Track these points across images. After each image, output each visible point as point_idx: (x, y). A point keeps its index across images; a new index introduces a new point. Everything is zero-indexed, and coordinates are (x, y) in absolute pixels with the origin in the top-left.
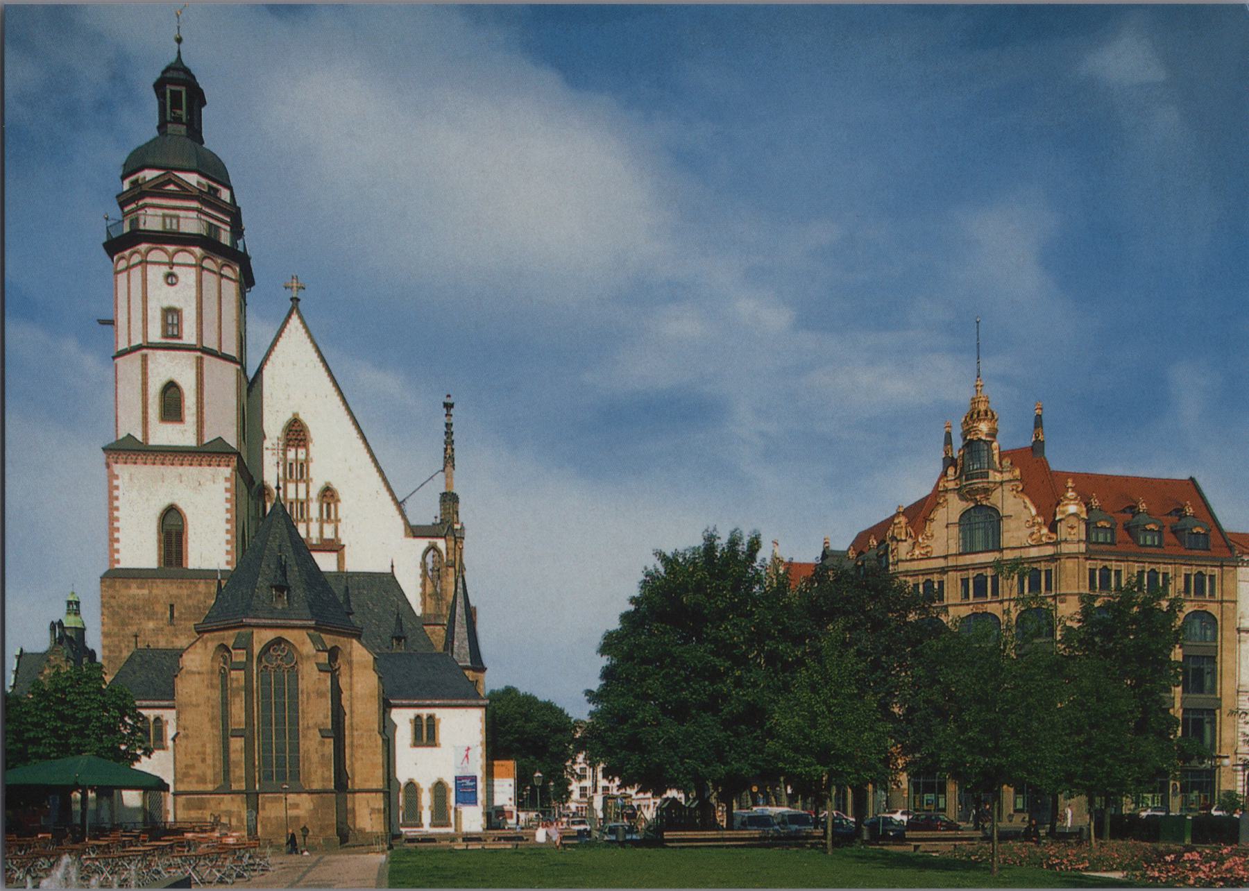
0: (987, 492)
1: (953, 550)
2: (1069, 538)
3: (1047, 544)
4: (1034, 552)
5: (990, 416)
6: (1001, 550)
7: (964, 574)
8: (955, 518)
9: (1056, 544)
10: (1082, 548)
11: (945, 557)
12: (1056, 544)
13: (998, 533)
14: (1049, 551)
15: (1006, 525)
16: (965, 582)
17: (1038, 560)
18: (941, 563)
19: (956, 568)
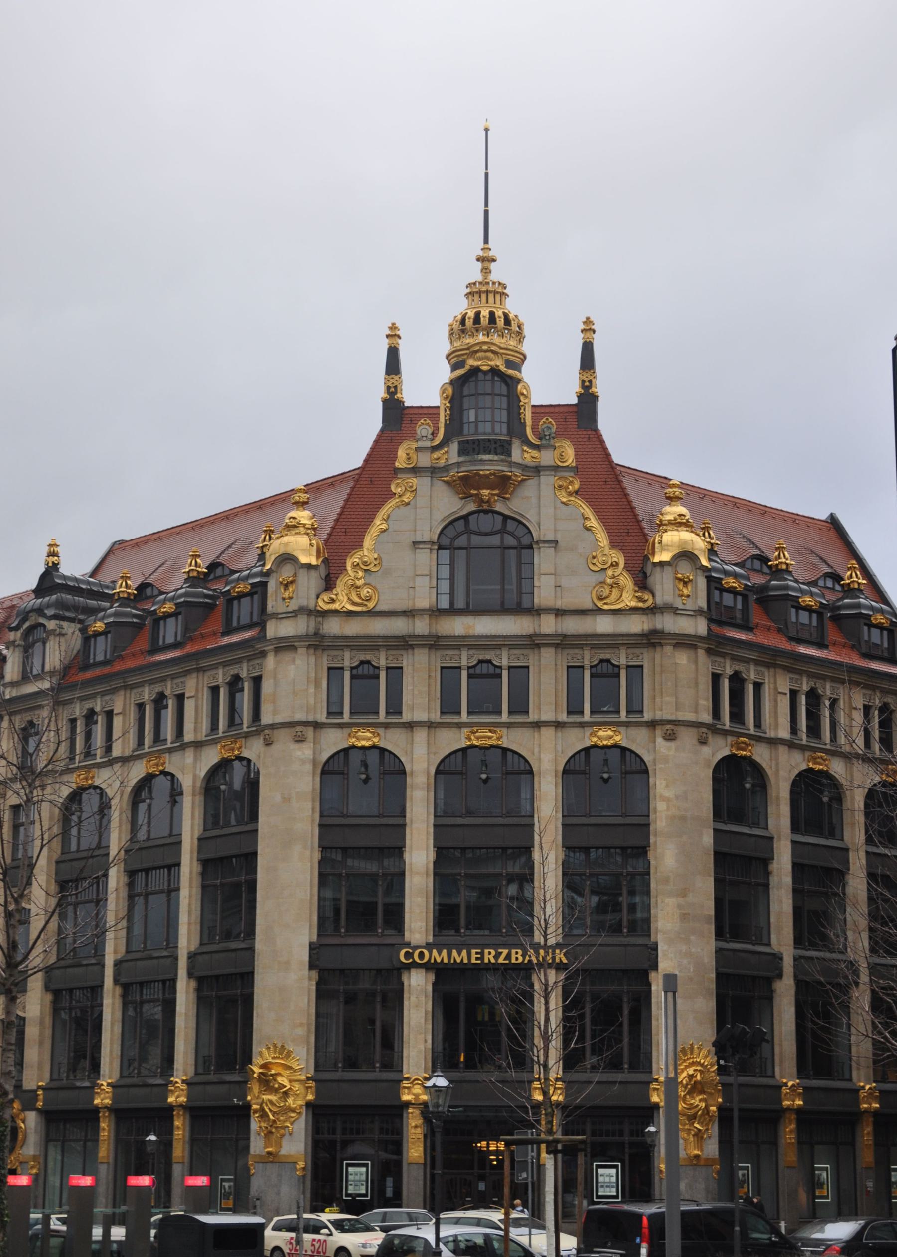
0: (503, 484)
1: (423, 602)
2: (678, 604)
3: (634, 610)
4: (604, 625)
5: (501, 322)
7: (450, 658)
9: (653, 610)
11: (410, 614)
12: (653, 610)
13: (525, 577)
14: (636, 625)
15: (543, 560)
16: (449, 673)
17: (614, 641)
18: (398, 626)
19: (435, 643)
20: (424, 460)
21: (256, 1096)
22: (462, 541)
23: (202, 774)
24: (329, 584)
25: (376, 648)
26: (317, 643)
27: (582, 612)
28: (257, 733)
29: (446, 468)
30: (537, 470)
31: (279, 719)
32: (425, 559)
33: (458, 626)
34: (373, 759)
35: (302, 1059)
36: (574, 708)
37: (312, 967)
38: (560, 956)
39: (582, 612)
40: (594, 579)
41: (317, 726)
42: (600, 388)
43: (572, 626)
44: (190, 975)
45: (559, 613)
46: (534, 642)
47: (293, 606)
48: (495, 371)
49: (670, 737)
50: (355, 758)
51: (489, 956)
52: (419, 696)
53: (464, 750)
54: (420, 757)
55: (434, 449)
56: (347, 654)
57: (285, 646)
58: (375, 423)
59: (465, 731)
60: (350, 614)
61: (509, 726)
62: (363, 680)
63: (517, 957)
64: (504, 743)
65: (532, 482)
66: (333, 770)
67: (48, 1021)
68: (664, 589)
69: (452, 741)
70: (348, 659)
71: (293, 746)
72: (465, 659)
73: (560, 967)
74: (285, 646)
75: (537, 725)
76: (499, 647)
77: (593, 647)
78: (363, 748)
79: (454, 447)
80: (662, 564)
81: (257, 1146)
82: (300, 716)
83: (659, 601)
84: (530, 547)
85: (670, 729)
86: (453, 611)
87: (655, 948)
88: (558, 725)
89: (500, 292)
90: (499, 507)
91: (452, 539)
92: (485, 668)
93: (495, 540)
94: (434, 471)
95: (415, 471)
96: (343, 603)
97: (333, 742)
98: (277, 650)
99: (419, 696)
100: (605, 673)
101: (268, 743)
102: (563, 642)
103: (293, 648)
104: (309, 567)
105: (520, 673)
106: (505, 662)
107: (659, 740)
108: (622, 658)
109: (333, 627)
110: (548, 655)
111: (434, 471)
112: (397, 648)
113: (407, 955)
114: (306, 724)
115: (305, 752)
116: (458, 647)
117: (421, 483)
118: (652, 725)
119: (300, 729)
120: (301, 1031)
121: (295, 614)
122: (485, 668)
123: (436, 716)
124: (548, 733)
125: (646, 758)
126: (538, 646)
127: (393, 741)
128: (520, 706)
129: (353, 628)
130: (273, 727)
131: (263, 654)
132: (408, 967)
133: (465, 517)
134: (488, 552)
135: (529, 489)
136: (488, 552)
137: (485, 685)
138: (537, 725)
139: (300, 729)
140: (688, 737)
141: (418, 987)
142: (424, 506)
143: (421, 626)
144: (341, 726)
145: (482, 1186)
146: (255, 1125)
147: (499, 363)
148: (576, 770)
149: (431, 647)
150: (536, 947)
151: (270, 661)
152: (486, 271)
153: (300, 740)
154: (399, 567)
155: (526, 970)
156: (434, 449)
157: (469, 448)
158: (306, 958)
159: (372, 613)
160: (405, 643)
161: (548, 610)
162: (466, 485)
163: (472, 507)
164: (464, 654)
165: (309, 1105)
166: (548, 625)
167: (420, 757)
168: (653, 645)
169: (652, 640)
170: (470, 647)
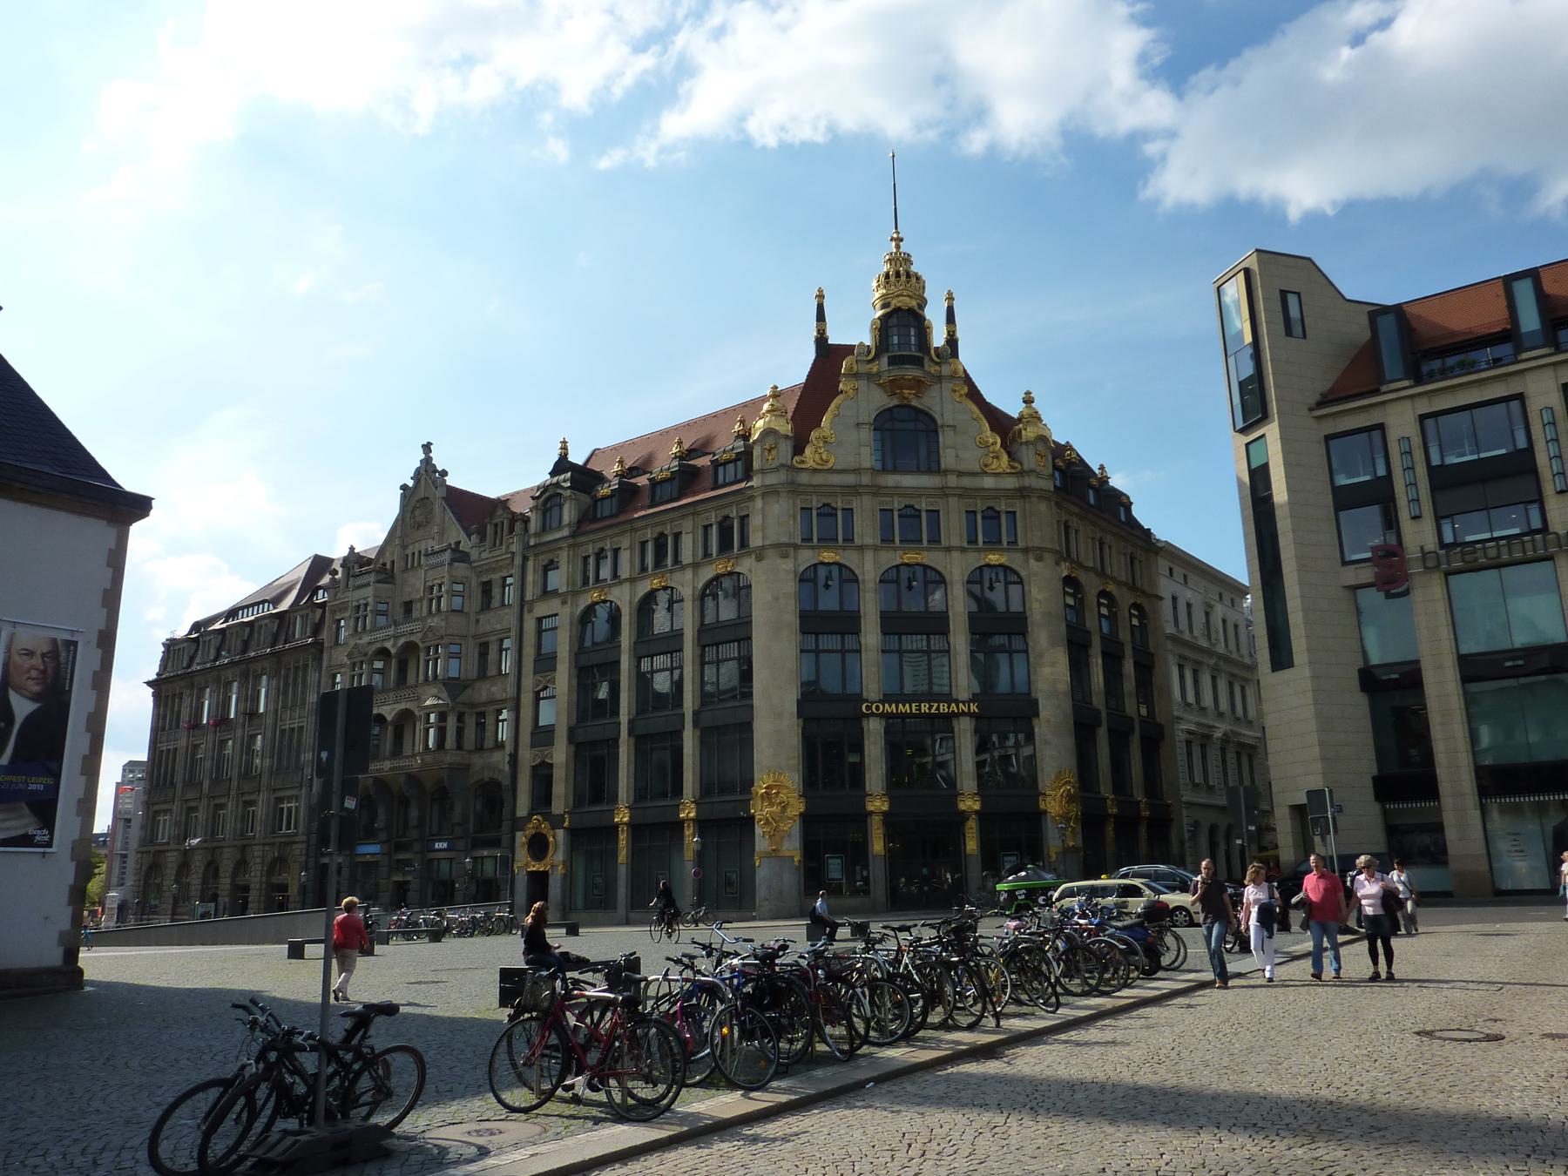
0: (918, 385)
1: (867, 464)
4: (988, 482)
6: (946, 472)
8: (868, 412)
9: (1021, 474)
10: (1048, 485)
14: (1010, 483)
15: (945, 438)
17: (997, 493)
18: (850, 479)
19: (877, 491)
20: (864, 368)
21: (760, 810)
22: (886, 426)
23: (700, 585)
24: (798, 450)
25: (834, 494)
26: (794, 489)
27: (974, 474)
28: (749, 554)
29: (879, 374)
30: (939, 378)
31: (767, 542)
32: (867, 435)
33: (891, 480)
34: (835, 571)
35: (792, 781)
36: (973, 541)
37: (799, 715)
38: (973, 708)
39: (974, 474)
40: (980, 452)
41: (796, 547)
42: (960, 334)
43: (967, 482)
44: (695, 726)
45: (960, 474)
46: (943, 493)
47: (776, 464)
48: (911, 311)
49: (1039, 559)
50: (822, 572)
51: (925, 708)
52: (866, 528)
53: (897, 567)
54: (869, 568)
55: (870, 362)
56: (814, 498)
57: (769, 492)
58: (810, 355)
59: (899, 553)
60: (815, 470)
61: (929, 550)
62: (825, 520)
63: (944, 708)
64: (926, 562)
65: (936, 387)
66: (807, 579)
67: (572, 765)
68: (1029, 458)
69: (891, 558)
70: (815, 502)
71: (779, 561)
72: (897, 504)
73: (969, 714)
74: (769, 492)
75: (949, 549)
76: (920, 496)
77: (983, 498)
78: (828, 564)
79: (885, 360)
80: (1027, 443)
81: (762, 844)
82: (784, 539)
83: (1026, 467)
84: (936, 432)
85: (1039, 553)
86: (884, 470)
87: (1036, 702)
88: (963, 550)
89: (907, 260)
90: (914, 403)
91: (885, 424)
92: (909, 511)
93: (911, 426)
94: (870, 377)
95: (857, 376)
96: (810, 464)
97: (807, 558)
98: (764, 495)
99: (866, 528)
100: (992, 515)
101: (759, 559)
102: (964, 493)
103: (777, 493)
104: (786, 437)
105: (934, 514)
106: (924, 506)
107: (1032, 561)
108: (1002, 506)
109: (804, 478)
110: (953, 501)
111: (870, 377)
112: (851, 494)
113: (868, 708)
114: (788, 545)
115: (787, 565)
116: (892, 495)
117: (862, 384)
118: (1026, 550)
119: (784, 549)
120: (793, 762)
121: (776, 470)
122: (909, 511)
123: (878, 542)
124: (956, 554)
125: (1023, 573)
126: (947, 496)
127: (849, 558)
128: (935, 539)
129: (818, 479)
130: (763, 547)
131: (752, 498)
132: (867, 716)
133: (890, 410)
134: (907, 433)
135: (934, 391)
136: (907, 433)
137: (910, 523)
138: (949, 549)
139: (784, 549)
140: (1049, 559)
141: (874, 729)
142: (857, 404)
143: (865, 479)
144: (813, 548)
145: (925, 871)
146: (758, 831)
147: (914, 303)
148: (976, 578)
149: (874, 494)
150: (957, 702)
151: (759, 503)
152: (898, 247)
153: (785, 556)
154: (844, 439)
155: (950, 717)
156: (870, 362)
157: (893, 361)
158: (795, 710)
159: (831, 471)
160: (854, 491)
161: (952, 471)
162: (893, 387)
163: (895, 402)
164: (896, 500)
165: (801, 815)
166: (952, 481)
167: (869, 568)
168: (1023, 497)
169: (1023, 493)
170: (901, 495)
